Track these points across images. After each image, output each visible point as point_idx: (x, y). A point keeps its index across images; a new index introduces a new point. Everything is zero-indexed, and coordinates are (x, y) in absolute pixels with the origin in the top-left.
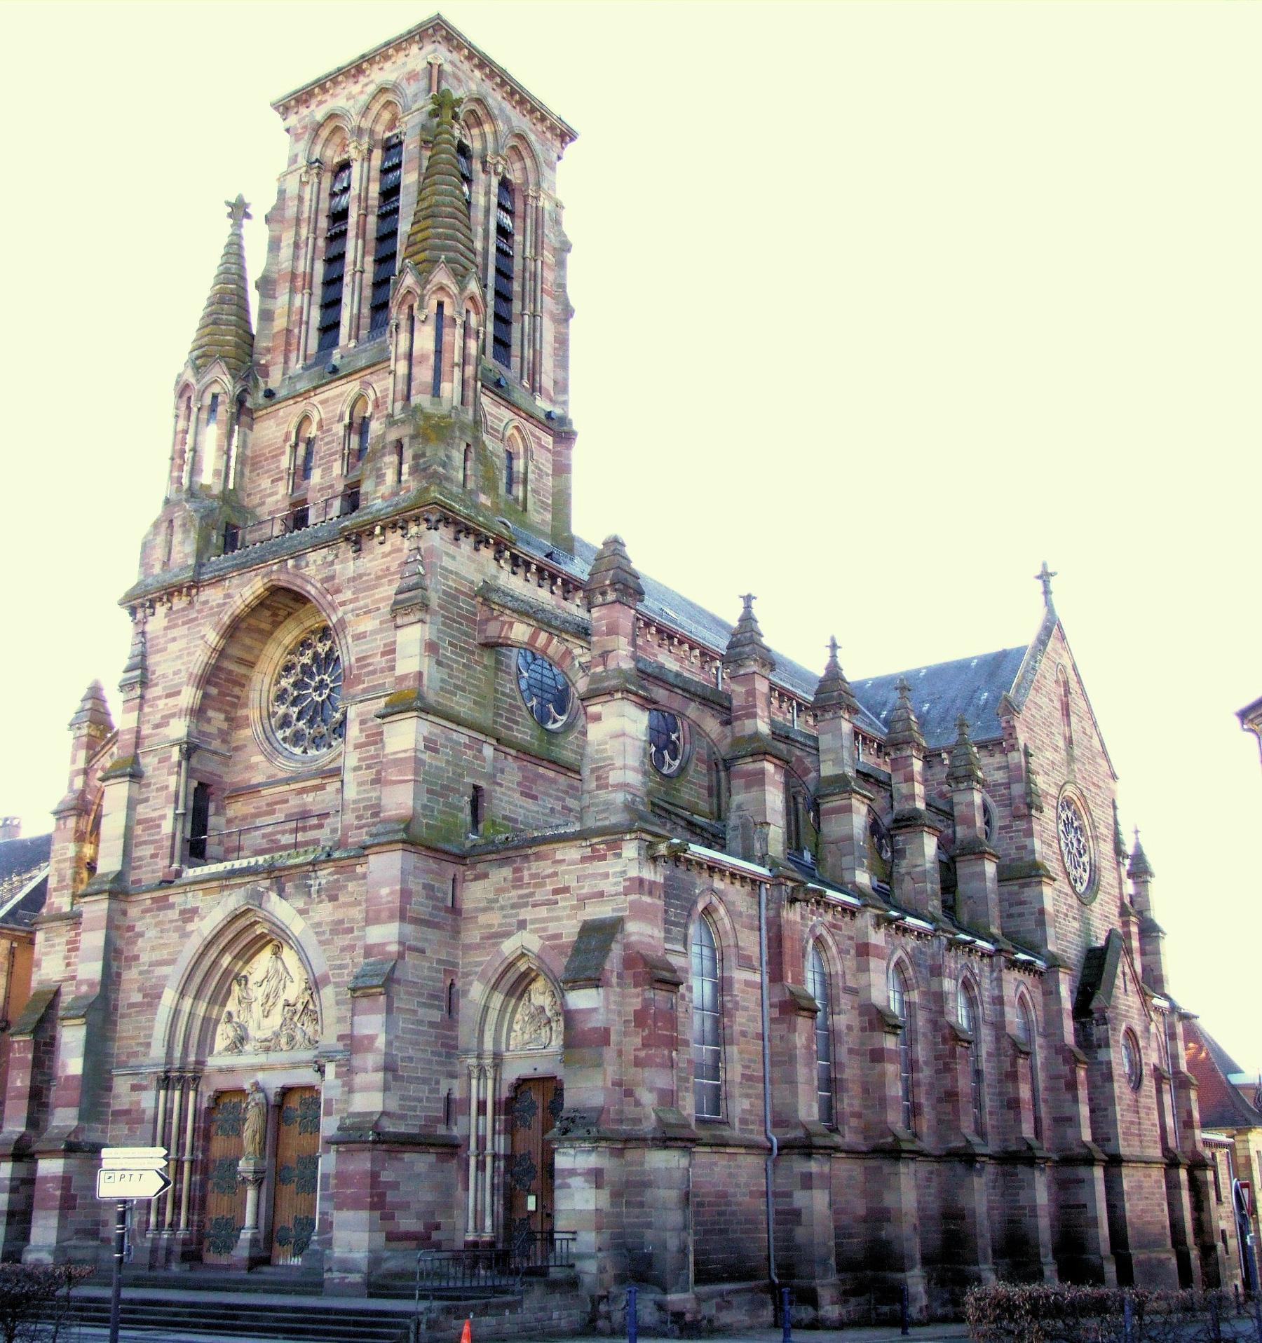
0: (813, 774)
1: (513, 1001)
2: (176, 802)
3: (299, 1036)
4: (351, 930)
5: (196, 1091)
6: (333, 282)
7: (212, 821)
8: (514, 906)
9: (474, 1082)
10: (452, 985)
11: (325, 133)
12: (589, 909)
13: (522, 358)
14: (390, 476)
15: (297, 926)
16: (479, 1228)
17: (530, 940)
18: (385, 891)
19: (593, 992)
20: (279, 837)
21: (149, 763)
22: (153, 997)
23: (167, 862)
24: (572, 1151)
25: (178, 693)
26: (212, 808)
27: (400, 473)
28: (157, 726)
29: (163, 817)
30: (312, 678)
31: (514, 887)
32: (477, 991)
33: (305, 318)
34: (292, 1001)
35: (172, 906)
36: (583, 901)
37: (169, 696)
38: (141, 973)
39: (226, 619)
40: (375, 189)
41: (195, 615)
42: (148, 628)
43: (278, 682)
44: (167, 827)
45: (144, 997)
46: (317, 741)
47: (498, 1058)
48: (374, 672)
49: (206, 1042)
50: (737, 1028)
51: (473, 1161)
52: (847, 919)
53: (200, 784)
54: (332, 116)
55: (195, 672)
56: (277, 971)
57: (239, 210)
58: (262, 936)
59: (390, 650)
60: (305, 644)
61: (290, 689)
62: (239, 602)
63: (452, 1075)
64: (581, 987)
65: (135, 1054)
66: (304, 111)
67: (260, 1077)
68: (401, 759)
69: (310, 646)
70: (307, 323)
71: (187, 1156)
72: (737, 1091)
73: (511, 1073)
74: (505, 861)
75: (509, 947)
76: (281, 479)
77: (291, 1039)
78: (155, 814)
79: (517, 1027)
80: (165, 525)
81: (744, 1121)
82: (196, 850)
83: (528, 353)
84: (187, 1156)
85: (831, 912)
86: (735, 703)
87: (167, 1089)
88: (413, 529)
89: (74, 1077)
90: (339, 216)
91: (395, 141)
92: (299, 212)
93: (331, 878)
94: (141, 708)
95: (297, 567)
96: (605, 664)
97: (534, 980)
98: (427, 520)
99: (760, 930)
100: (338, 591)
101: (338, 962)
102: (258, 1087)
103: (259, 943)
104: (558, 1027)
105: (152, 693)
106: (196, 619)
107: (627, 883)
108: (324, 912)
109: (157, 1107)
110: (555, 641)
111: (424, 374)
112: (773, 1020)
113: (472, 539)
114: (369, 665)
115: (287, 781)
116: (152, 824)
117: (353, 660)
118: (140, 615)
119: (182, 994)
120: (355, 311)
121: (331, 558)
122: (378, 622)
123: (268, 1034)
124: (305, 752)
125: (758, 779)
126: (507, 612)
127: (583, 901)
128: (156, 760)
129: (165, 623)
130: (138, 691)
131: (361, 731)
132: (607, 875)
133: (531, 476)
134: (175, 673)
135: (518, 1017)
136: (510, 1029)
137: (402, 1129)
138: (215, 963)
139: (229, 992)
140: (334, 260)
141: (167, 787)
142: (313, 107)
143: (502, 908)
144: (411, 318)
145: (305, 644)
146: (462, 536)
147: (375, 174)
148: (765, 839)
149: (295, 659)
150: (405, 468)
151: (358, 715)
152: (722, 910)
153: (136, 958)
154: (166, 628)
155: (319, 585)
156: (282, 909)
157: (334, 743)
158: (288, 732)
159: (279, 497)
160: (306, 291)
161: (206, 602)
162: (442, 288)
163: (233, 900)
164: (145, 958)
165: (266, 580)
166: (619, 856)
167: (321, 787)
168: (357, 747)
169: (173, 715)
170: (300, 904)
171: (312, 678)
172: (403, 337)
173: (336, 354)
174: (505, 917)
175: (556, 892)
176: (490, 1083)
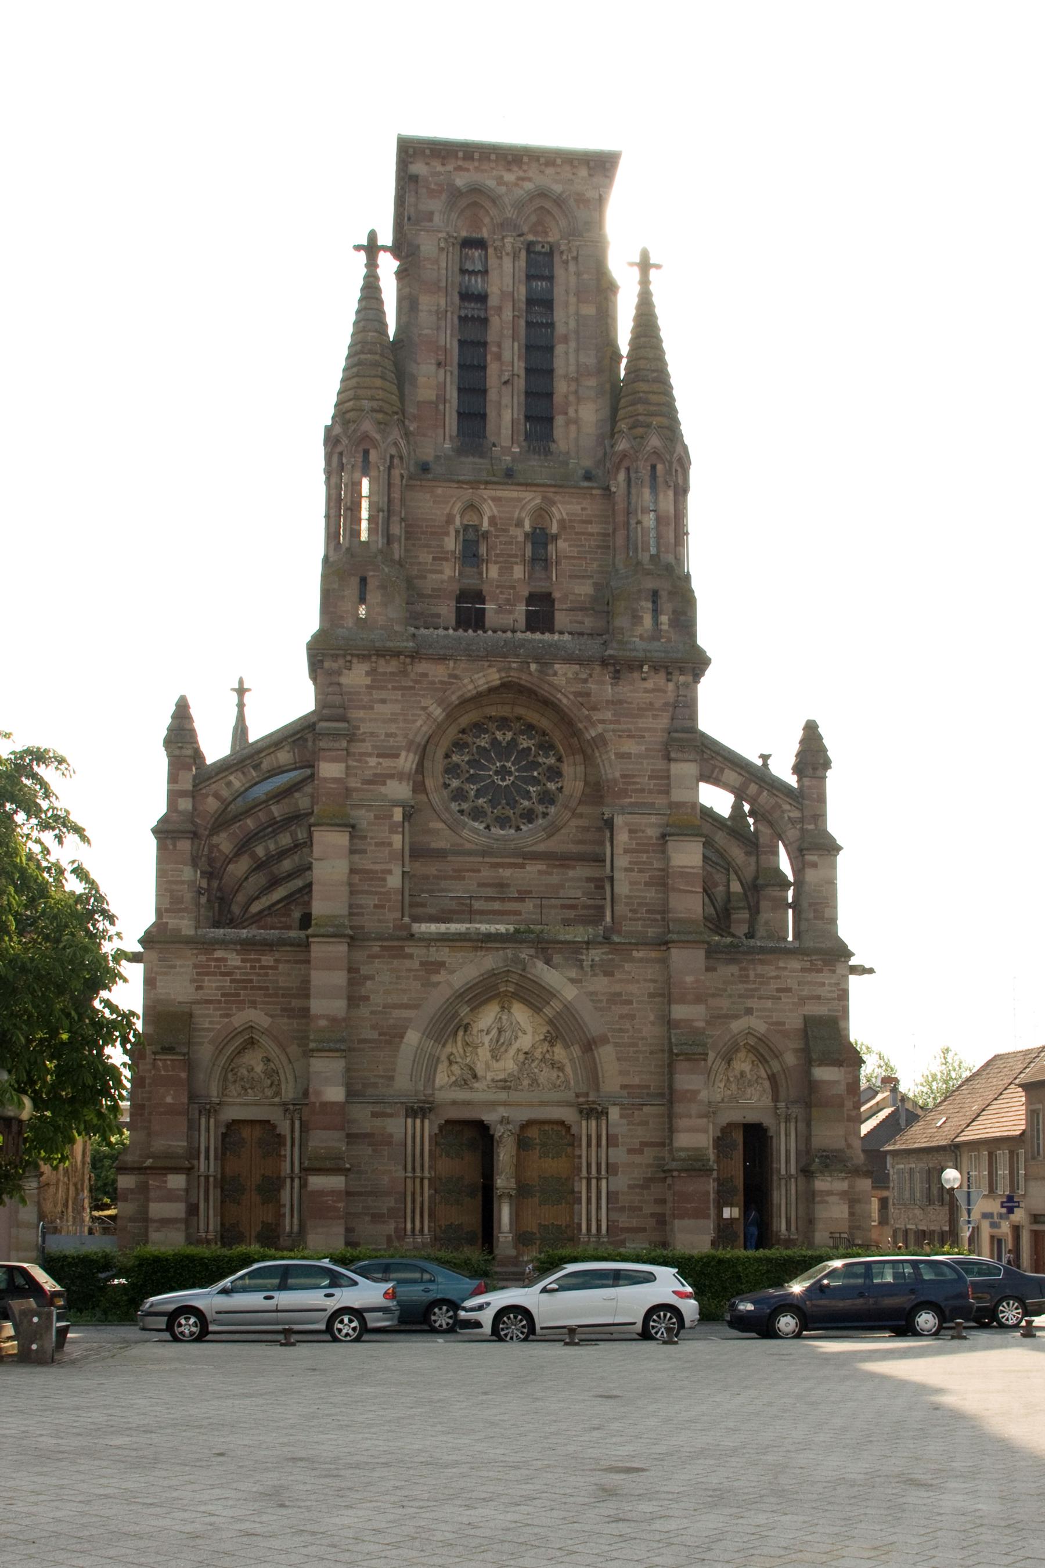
4: (630, 1002)
8: (740, 996)
12: (807, 1008)
22: (393, 1036)
23: (398, 915)
29: (390, 872)
31: (742, 982)
35: (410, 956)
36: (803, 1000)
38: (372, 1013)
39: (454, 698)
41: (411, 684)
46: (503, 822)
48: (642, 791)
55: (418, 739)
62: (470, 687)
64: (827, 1065)
65: (375, 1085)
68: (690, 873)
69: (486, 731)
74: (732, 961)
75: (737, 1026)
77: (534, 1082)
93: (605, 957)
94: (346, 762)
96: (816, 825)
100: (594, 708)
101: (618, 1027)
106: (413, 688)
108: (600, 984)
110: (765, 793)
114: (637, 783)
115: (484, 853)
116: (378, 877)
117: (617, 774)
121: (584, 676)
122: (643, 748)
126: (720, 758)
127: (803, 1000)
128: (372, 815)
131: (631, 838)
132: (823, 984)
134: (388, 735)
141: (390, 844)
143: (730, 996)
151: (627, 824)
153: (367, 998)
158: (465, 806)
161: (426, 675)
164: (377, 999)
165: (503, 675)
166: (834, 972)
167: (522, 866)
169: (391, 776)
170: (573, 974)
174: (733, 1003)
175: (778, 990)
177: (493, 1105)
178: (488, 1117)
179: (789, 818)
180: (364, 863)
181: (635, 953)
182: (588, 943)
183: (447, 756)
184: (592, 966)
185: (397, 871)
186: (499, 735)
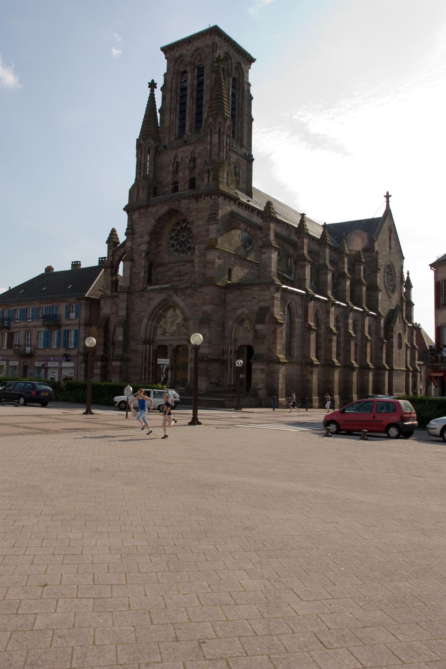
0: (317, 263)
1: (240, 325)
2: (144, 268)
3: (181, 332)
4: (197, 306)
5: (153, 345)
6: (183, 111)
7: (153, 273)
8: (240, 301)
9: (229, 346)
10: (224, 321)
11: (179, 61)
13: (238, 136)
14: (206, 180)
15: (182, 304)
16: (230, 382)
17: (245, 310)
18: (208, 297)
19: (263, 325)
20: (173, 278)
21: (136, 257)
22: (140, 320)
23: (143, 284)
24: (256, 364)
25: (144, 237)
26: (153, 269)
27: (209, 179)
28: (137, 246)
29: (141, 272)
30: (180, 233)
32: (230, 323)
33: (174, 123)
34: (179, 323)
35: (145, 297)
37: (140, 238)
39: (157, 217)
40: (195, 82)
42: (133, 217)
43: (170, 234)
44: (142, 275)
45: (138, 320)
46: (183, 252)
47: (235, 340)
48: (202, 236)
49: (155, 333)
50: (296, 334)
51: (229, 365)
52: (325, 304)
53: (150, 263)
54: (181, 56)
56: (175, 315)
57: (152, 85)
58: (171, 305)
59: (207, 231)
60: (178, 224)
61: (174, 236)
62: (161, 212)
63: (224, 344)
64: (259, 324)
66: (172, 53)
67: (171, 342)
69: (180, 224)
70: (175, 124)
71: (151, 362)
72: (295, 350)
73: (239, 344)
75: (239, 312)
76: (170, 174)
77: (179, 333)
78: (139, 271)
79: (240, 332)
80: (136, 187)
81: (297, 357)
82: (150, 281)
83: (240, 134)
84: (151, 362)
85: (320, 302)
86: (298, 245)
87: (145, 345)
88: (213, 197)
89: (120, 341)
90: (184, 89)
91: (201, 66)
92: (172, 87)
93: (191, 292)
94: (132, 241)
95: (178, 204)
96: (266, 238)
97: (245, 320)
98: (218, 195)
99: (303, 308)
100: (191, 212)
102: (170, 345)
103: (170, 307)
104: (252, 332)
105: (136, 236)
106: (148, 216)
107: (271, 297)
109: (143, 349)
110: (252, 230)
111: (215, 150)
112: (305, 332)
113: (229, 199)
114: (201, 234)
115: (175, 263)
117: (196, 232)
118: (130, 213)
119: (149, 320)
120: (191, 123)
121: (189, 202)
122: (203, 222)
123: (173, 331)
124: (179, 254)
125: (304, 267)
126: (239, 220)
128: (138, 256)
129: (138, 216)
130: (131, 236)
131: (199, 252)
132: (266, 295)
133: (241, 174)
134: (142, 231)
135: (241, 329)
136: (238, 333)
137: (213, 357)
138: (158, 312)
139: (161, 319)
140: (183, 104)
141: (141, 264)
142: (175, 52)
144: (211, 132)
145: (178, 224)
146: (226, 198)
147: (195, 77)
148: (305, 283)
149: (175, 228)
150: (211, 178)
152: (293, 303)
153: (135, 310)
154: (139, 218)
155: (185, 210)
156: (177, 299)
157: (188, 253)
158: (174, 248)
159: (169, 179)
160: (175, 114)
161: (151, 211)
162: (220, 123)
163: (163, 296)
165: (169, 207)
166: (269, 290)
167: (185, 265)
168: (198, 257)
169: (142, 243)
170: (183, 298)
171: (180, 233)
172: (209, 138)
173: (185, 137)
175: (252, 298)
176: (233, 346)
177: (169, 340)
178: (167, 344)
179: (259, 237)
180: (134, 270)
181: (199, 290)
182: (186, 288)
183: (170, 234)
184: (188, 295)
185: (143, 271)
186: (183, 225)
